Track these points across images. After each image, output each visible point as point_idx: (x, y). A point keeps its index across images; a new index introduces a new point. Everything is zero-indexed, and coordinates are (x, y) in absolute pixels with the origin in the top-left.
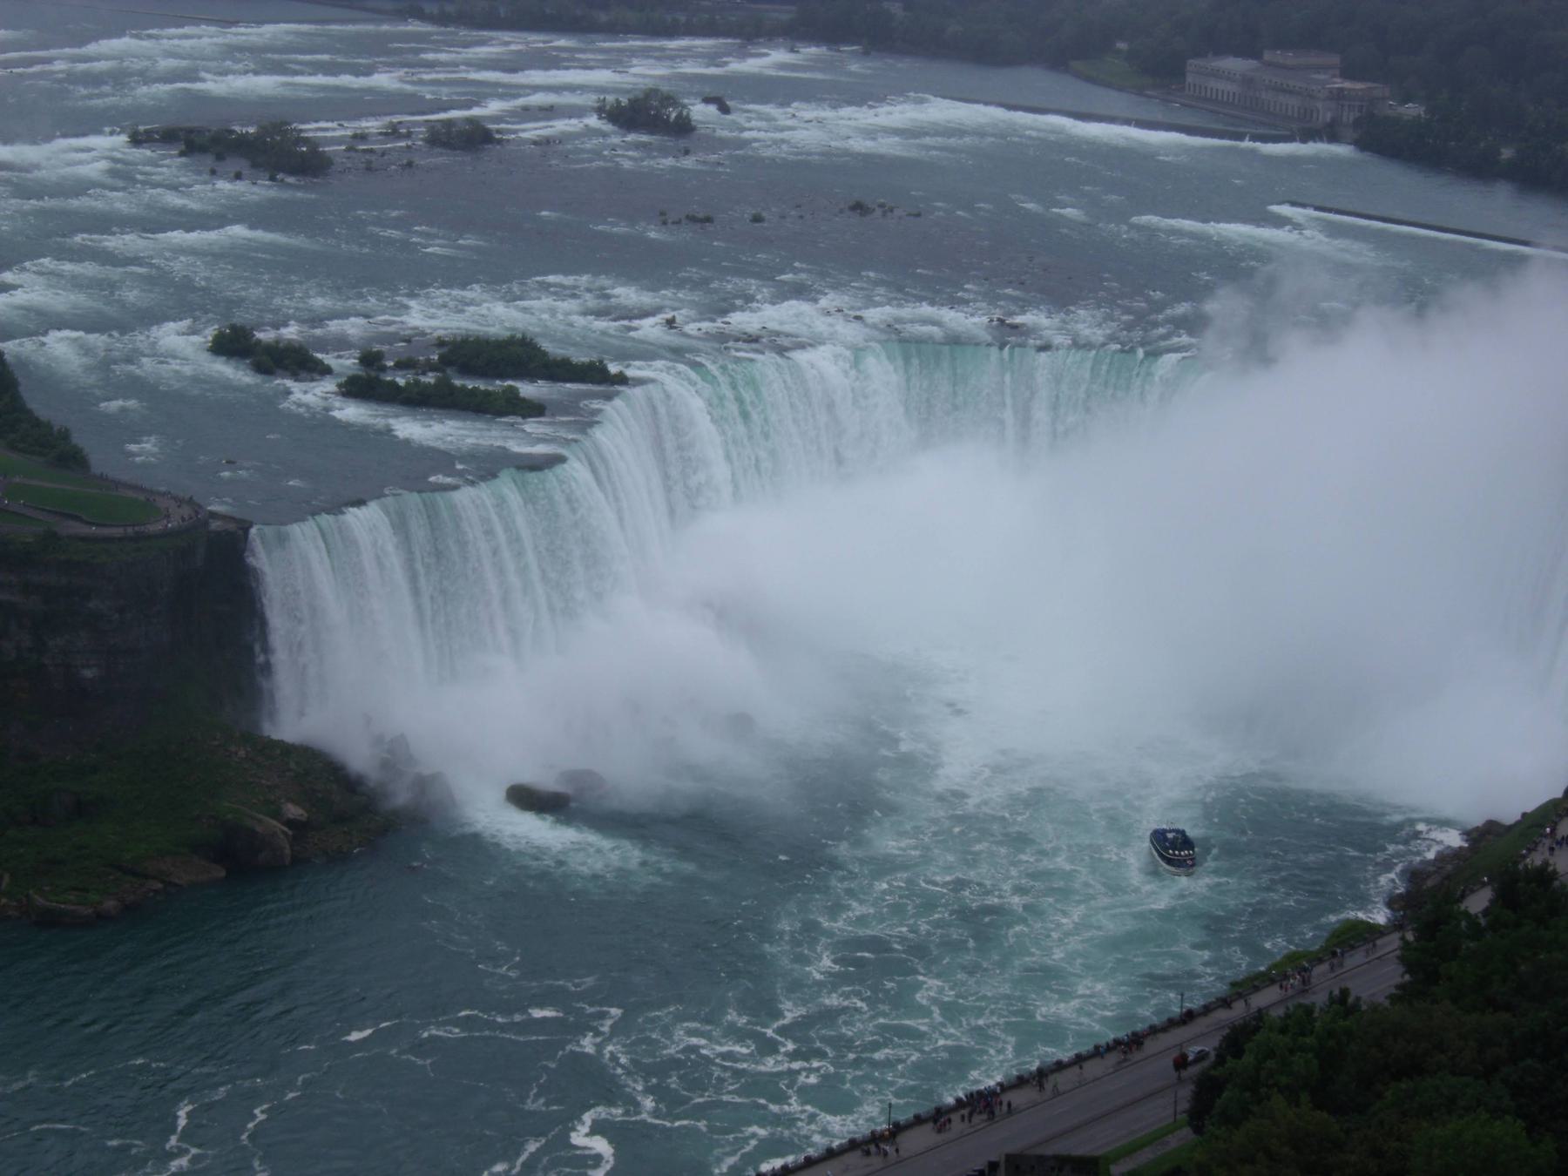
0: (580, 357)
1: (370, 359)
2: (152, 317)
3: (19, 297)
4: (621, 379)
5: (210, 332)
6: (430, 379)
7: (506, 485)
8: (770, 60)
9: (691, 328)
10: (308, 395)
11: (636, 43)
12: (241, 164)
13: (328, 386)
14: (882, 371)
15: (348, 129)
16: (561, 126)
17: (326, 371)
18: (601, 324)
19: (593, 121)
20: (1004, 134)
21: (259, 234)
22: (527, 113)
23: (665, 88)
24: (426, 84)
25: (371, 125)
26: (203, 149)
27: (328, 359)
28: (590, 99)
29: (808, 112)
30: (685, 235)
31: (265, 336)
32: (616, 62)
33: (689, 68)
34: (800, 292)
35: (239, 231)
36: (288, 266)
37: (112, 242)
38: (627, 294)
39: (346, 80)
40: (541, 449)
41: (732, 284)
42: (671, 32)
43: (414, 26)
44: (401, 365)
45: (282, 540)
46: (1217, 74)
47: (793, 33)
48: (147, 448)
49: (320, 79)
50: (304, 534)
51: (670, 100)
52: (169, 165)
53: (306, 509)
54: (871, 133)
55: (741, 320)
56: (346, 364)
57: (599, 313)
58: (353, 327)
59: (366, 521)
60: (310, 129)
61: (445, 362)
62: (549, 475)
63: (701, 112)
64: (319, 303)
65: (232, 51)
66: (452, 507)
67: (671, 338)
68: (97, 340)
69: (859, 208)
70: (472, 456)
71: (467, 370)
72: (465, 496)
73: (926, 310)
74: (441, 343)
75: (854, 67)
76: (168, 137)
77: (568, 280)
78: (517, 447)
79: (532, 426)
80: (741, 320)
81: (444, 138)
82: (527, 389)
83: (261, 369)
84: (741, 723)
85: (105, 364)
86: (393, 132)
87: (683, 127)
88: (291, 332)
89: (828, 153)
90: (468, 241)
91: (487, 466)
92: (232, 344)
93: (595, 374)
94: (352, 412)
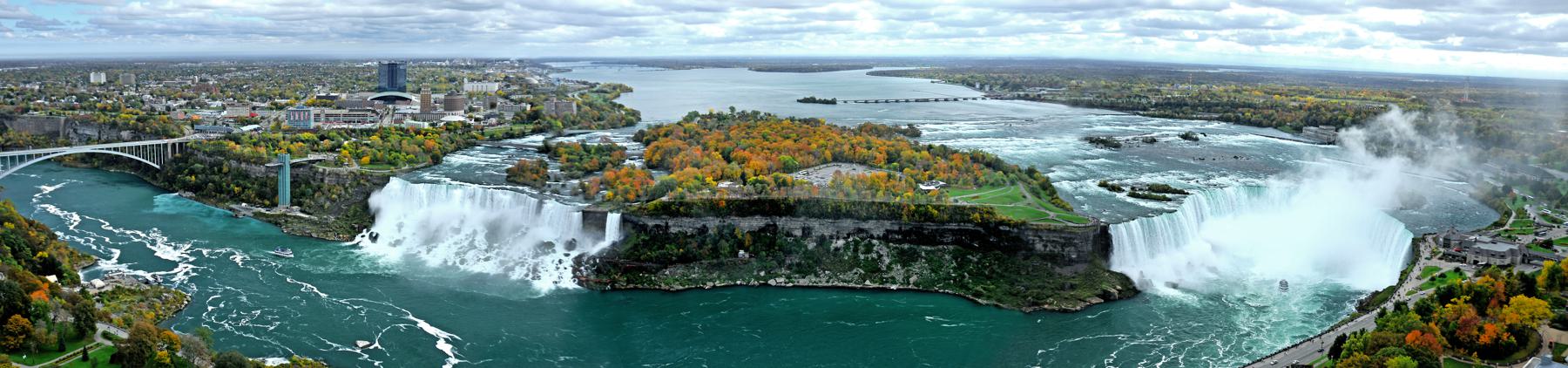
0: (1179, 188)
1: (1133, 188)
2: (1084, 178)
3: (1056, 173)
4: (1188, 194)
5: (1098, 182)
6: (1146, 193)
7: (1164, 214)
8: (1215, 125)
9: (1201, 182)
10: (1120, 196)
11: (1184, 121)
12: (1103, 145)
13: (1125, 194)
14: (1243, 194)
15: (1125, 138)
16: (1170, 139)
17: (1124, 190)
18: (1183, 181)
19: (1177, 137)
20: (1264, 142)
21: (1107, 161)
22: (1163, 136)
23: (1193, 131)
24: (1140, 129)
25: (1130, 137)
26: (1094, 142)
27: (1124, 188)
28: (1177, 133)
29: (1225, 136)
30: (1199, 163)
31: (1110, 183)
32: (1181, 125)
33: (1198, 126)
34: (1225, 175)
35: (1103, 160)
36: (1114, 168)
37: (1075, 162)
38: (1187, 175)
39: (1124, 128)
40: (1172, 208)
41: (1210, 173)
42: (1193, 119)
43: (1138, 116)
44: (1140, 190)
45: (1117, 228)
46: (1309, 130)
47: (1220, 119)
48: (1086, 207)
49: (1117, 127)
50: (1121, 226)
51: (1194, 134)
52: (1088, 145)
53: (1119, 221)
54: (1237, 142)
55: (1212, 181)
56: (1128, 189)
57: (1182, 179)
58: (1129, 181)
59: (1134, 224)
60: (1117, 138)
61: (1150, 189)
62: (1173, 214)
63: (1200, 136)
64: (1122, 176)
65: (1099, 121)
66: (1153, 222)
67: (1198, 185)
68: (1074, 183)
69: (1235, 157)
70: (1157, 210)
71: (1154, 191)
72: (1155, 218)
73: (1252, 180)
74: (1148, 185)
75: (1232, 127)
76: (1086, 139)
77: (1174, 172)
78: (1166, 208)
79: (1169, 203)
80: (1212, 181)
81: (1145, 141)
82: (1169, 195)
83: (1109, 190)
84: (1213, 270)
85: (1076, 188)
86: (1134, 139)
87: (1197, 139)
88: (1116, 182)
89: (1228, 145)
90: (1153, 163)
91: (1160, 212)
92: (1103, 185)
93: (1181, 192)
94: (1130, 200)
